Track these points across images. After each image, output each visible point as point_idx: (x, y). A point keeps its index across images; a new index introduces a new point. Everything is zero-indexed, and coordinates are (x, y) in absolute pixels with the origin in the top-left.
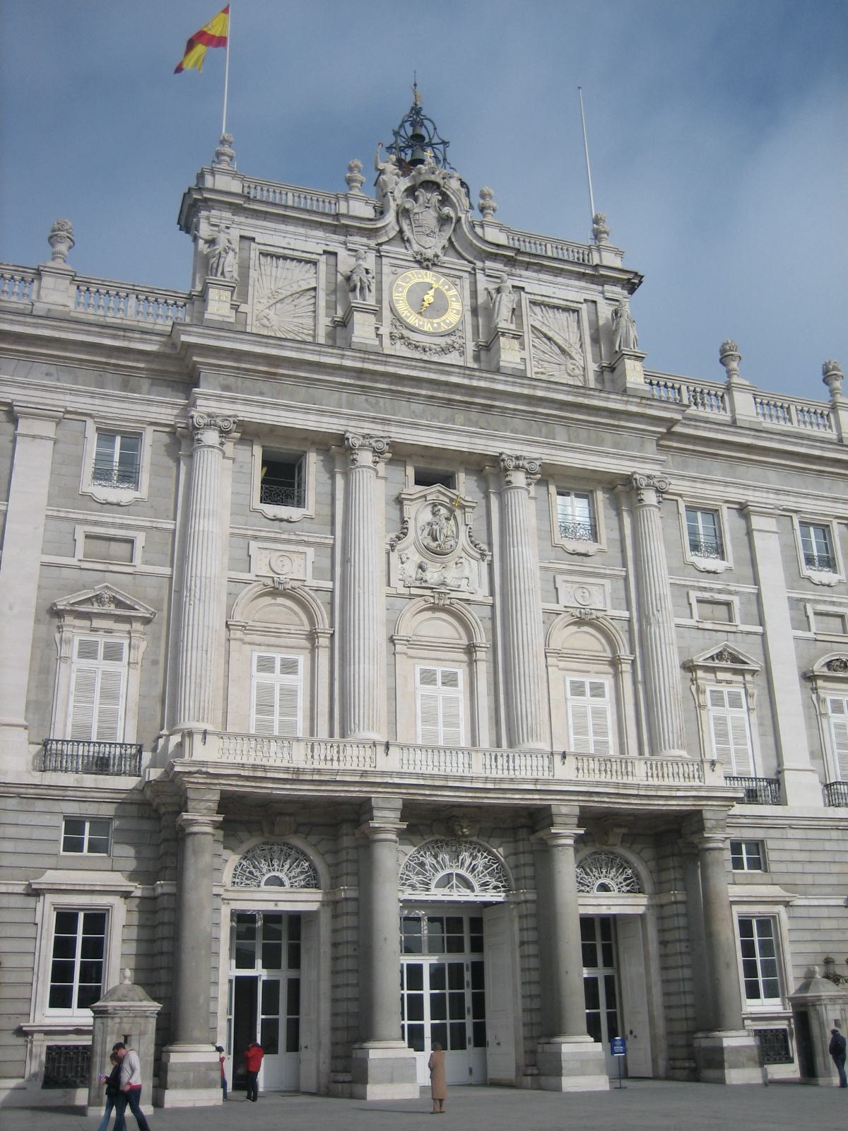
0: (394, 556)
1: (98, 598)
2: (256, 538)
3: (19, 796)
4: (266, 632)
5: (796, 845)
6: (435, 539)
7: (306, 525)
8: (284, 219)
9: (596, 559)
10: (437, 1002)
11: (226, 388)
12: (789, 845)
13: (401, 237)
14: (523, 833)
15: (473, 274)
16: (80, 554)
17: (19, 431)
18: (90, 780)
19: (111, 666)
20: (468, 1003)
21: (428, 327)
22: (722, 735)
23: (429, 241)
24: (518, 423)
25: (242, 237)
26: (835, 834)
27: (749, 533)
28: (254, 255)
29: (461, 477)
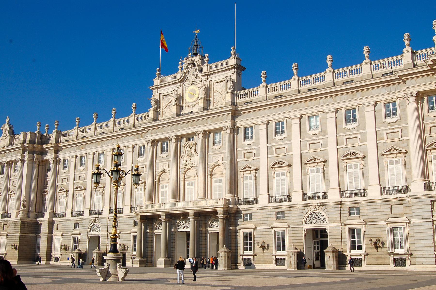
5: (259, 214)
8: (166, 86)
11: (151, 133)
12: (257, 214)
15: (201, 81)
21: (192, 101)
22: (246, 188)
24: (201, 122)
25: (160, 94)
26: (269, 210)
28: (162, 97)
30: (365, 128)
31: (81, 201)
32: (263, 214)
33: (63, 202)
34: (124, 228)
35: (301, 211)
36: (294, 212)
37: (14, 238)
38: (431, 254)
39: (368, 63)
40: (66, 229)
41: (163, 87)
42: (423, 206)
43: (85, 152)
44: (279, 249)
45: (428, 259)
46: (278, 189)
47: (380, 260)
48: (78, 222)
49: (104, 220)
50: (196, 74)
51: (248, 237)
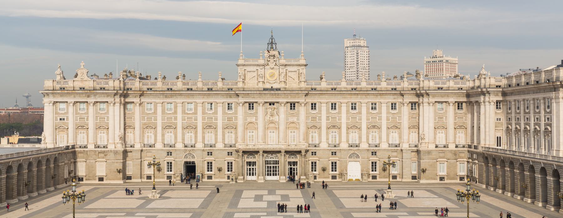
0: (266, 117)
2: (248, 116)
4: (250, 128)
5: (321, 152)
7: (254, 114)
9: (295, 114)
11: (242, 97)
12: (320, 152)
16: (227, 120)
17: (218, 105)
18: (230, 148)
19: (231, 134)
20: (277, 171)
22: (312, 137)
23: (272, 64)
24: (283, 96)
25: (244, 70)
26: (328, 151)
28: (246, 72)
29: (275, 104)
30: (381, 114)
31: (171, 136)
33: (151, 136)
34: (218, 157)
35: (346, 152)
36: (342, 152)
37: (116, 164)
38: (409, 174)
39: (385, 81)
41: (247, 66)
42: (408, 154)
44: (332, 171)
45: (408, 177)
47: (385, 176)
48: (171, 151)
49: (199, 151)
50: (275, 62)
51: (314, 164)
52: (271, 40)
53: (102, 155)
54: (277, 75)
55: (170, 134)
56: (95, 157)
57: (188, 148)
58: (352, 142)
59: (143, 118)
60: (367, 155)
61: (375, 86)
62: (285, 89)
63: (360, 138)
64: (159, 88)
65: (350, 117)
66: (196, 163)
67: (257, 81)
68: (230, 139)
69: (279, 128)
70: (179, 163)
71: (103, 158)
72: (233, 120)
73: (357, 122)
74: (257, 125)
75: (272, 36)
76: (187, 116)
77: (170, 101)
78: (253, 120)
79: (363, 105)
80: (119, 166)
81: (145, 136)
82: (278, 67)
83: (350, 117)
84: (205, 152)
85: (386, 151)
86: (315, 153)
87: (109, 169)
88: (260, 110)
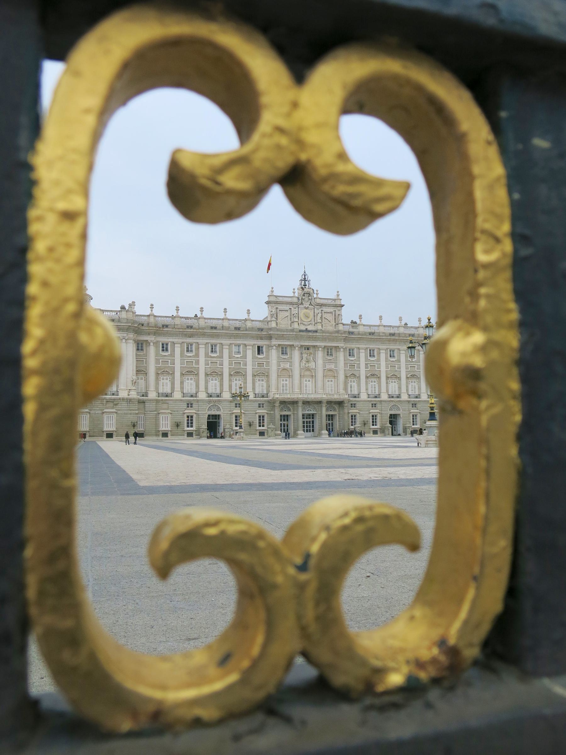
1: (260, 373)
2: (281, 362)
3: (253, 401)
4: (283, 375)
5: (361, 404)
6: (307, 359)
7: (288, 359)
8: (283, 304)
10: (307, 426)
11: (276, 339)
12: (360, 404)
13: (302, 304)
14: (319, 404)
15: (314, 309)
18: (262, 399)
19: (262, 382)
20: (311, 426)
21: (307, 321)
22: (351, 387)
26: (368, 402)
27: (360, 352)
28: (278, 311)
31: (191, 384)
32: (363, 404)
33: (167, 383)
34: (248, 409)
36: (383, 404)
40: (175, 407)
41: (280, 304)
43: (195, 341)
46: (372, 390)
48: (192, 402)
49: (226, 402)
50: (310, 302)
51: (353, 417)
52: (303, 276)
53: (111, 405)
54: (312, 315)
55: (190, 381)
56: (102, 406)
57: (214, 398)
58: (392, 392)
59: (157, 361)
60: (408, 407)
61: (413, 333)
62: (323, 332)
63: (400, 388)
64: (177, 324)
65: (389, 366)
66: (222, 416)
67: (290, 322)
68: (261, 387)
69: (315, 376)
70: (201, 416)
71: (113, 408)
72: (263, 366)
73: (396, 371)
74: (292, 372)
75: (305, 272)
76: (210, 360)
77: (191, 341)
78: (287, 366)
79: (401, 352)
80: (133, 418)
81: (160, 384)
82: (313, 306)
83: (389, 365)
84: (232, 404)
85: (426, 403)
86: (355, 404)
87: (120, 422)
88: (296, 354)
